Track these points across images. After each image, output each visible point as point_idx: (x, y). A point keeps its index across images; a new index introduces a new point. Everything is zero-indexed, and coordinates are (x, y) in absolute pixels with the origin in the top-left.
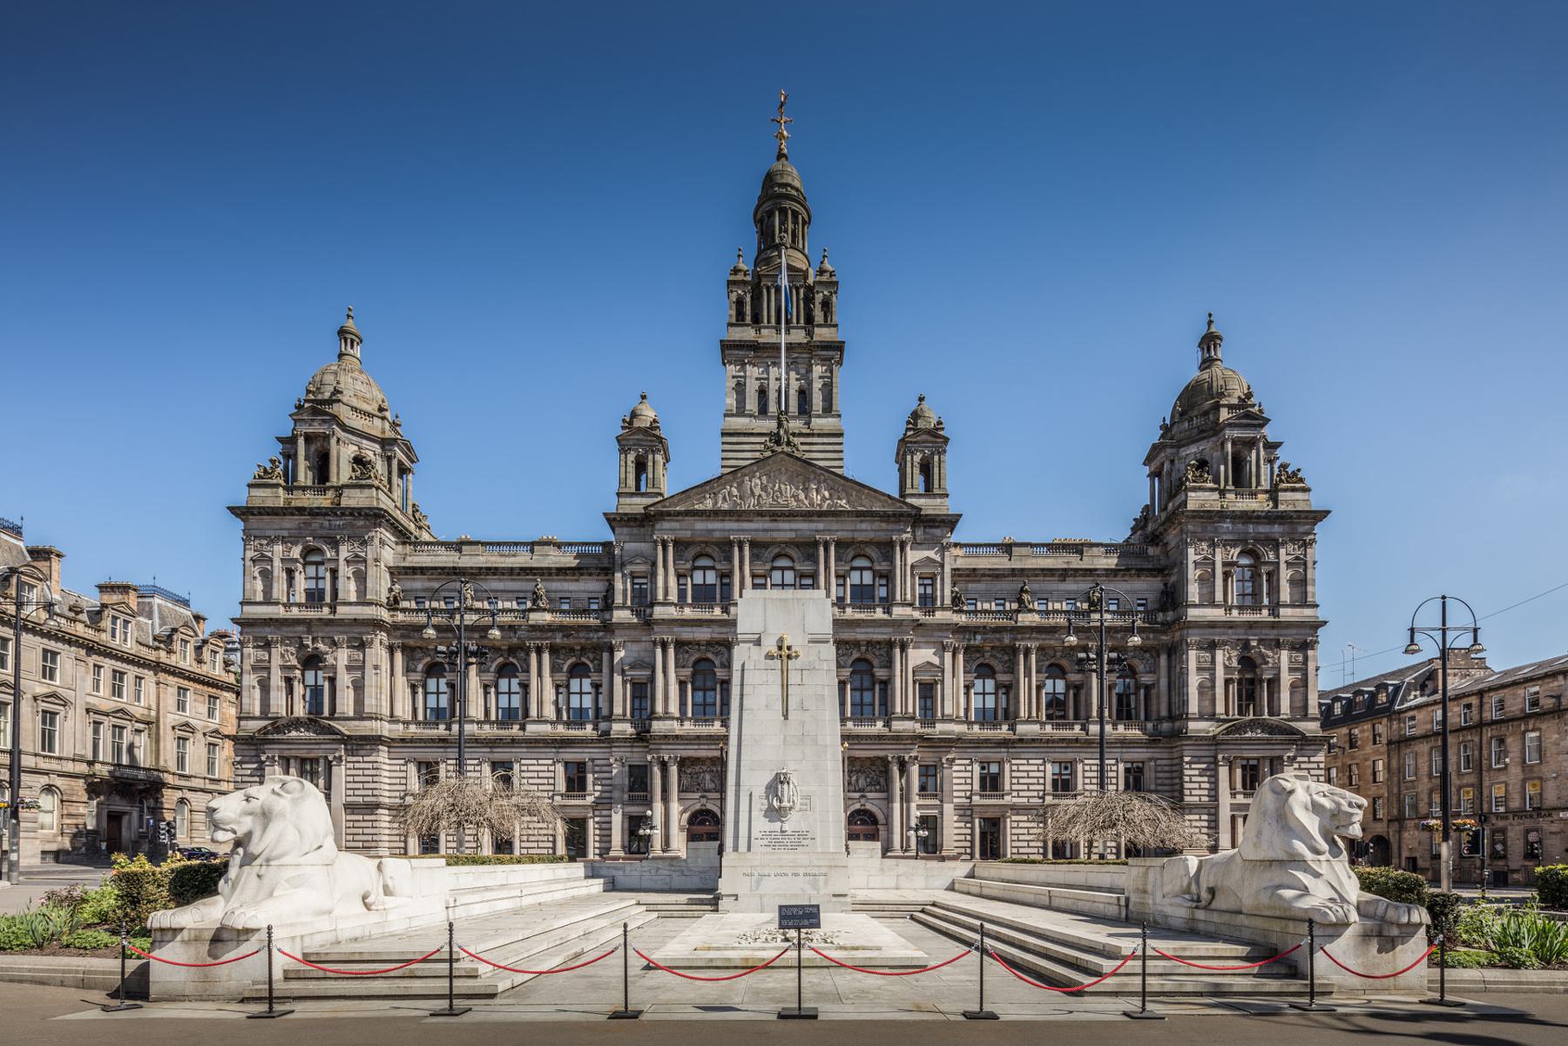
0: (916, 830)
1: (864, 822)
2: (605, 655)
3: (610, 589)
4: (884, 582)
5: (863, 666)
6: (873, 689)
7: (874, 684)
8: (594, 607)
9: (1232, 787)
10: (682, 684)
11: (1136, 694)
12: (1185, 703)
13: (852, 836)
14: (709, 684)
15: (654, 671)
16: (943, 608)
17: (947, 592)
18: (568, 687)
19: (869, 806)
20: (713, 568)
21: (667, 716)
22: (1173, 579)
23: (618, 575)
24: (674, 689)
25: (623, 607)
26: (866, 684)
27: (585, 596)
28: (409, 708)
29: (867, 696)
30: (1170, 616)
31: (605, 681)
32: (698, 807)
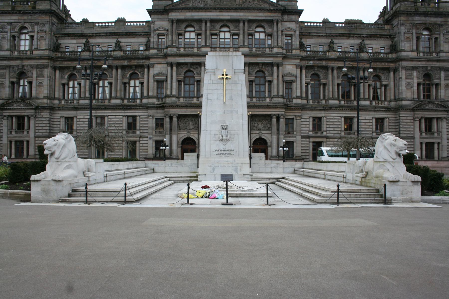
0: (283, 148)
1: (261, 144)
2: (146, 70)
3: (149, 41)
4: (270, 38)
5: (261, 74)
6: (265, 85)
7: (265, 82)
8: (141, 49)
9: (420, 130)
10: (179, 82)
11: (381, 89)
12: (401, 93)
13: (256, 151)
14: (192, 82)
15: (167, 76)
16: (296, 49)
17: (298, 43)
18: (129, 83)
19: (263, 137)
20: (194, 31)
21: (171, 96)
22: (396, 39)
23: (152, 35)
24: (175, 84)
25: (154, 49)
27: (138, 44)
28: (61, 94)
29: (262, 88)
30: (393, 56)
31: (145, 81)
32: (186, 137)
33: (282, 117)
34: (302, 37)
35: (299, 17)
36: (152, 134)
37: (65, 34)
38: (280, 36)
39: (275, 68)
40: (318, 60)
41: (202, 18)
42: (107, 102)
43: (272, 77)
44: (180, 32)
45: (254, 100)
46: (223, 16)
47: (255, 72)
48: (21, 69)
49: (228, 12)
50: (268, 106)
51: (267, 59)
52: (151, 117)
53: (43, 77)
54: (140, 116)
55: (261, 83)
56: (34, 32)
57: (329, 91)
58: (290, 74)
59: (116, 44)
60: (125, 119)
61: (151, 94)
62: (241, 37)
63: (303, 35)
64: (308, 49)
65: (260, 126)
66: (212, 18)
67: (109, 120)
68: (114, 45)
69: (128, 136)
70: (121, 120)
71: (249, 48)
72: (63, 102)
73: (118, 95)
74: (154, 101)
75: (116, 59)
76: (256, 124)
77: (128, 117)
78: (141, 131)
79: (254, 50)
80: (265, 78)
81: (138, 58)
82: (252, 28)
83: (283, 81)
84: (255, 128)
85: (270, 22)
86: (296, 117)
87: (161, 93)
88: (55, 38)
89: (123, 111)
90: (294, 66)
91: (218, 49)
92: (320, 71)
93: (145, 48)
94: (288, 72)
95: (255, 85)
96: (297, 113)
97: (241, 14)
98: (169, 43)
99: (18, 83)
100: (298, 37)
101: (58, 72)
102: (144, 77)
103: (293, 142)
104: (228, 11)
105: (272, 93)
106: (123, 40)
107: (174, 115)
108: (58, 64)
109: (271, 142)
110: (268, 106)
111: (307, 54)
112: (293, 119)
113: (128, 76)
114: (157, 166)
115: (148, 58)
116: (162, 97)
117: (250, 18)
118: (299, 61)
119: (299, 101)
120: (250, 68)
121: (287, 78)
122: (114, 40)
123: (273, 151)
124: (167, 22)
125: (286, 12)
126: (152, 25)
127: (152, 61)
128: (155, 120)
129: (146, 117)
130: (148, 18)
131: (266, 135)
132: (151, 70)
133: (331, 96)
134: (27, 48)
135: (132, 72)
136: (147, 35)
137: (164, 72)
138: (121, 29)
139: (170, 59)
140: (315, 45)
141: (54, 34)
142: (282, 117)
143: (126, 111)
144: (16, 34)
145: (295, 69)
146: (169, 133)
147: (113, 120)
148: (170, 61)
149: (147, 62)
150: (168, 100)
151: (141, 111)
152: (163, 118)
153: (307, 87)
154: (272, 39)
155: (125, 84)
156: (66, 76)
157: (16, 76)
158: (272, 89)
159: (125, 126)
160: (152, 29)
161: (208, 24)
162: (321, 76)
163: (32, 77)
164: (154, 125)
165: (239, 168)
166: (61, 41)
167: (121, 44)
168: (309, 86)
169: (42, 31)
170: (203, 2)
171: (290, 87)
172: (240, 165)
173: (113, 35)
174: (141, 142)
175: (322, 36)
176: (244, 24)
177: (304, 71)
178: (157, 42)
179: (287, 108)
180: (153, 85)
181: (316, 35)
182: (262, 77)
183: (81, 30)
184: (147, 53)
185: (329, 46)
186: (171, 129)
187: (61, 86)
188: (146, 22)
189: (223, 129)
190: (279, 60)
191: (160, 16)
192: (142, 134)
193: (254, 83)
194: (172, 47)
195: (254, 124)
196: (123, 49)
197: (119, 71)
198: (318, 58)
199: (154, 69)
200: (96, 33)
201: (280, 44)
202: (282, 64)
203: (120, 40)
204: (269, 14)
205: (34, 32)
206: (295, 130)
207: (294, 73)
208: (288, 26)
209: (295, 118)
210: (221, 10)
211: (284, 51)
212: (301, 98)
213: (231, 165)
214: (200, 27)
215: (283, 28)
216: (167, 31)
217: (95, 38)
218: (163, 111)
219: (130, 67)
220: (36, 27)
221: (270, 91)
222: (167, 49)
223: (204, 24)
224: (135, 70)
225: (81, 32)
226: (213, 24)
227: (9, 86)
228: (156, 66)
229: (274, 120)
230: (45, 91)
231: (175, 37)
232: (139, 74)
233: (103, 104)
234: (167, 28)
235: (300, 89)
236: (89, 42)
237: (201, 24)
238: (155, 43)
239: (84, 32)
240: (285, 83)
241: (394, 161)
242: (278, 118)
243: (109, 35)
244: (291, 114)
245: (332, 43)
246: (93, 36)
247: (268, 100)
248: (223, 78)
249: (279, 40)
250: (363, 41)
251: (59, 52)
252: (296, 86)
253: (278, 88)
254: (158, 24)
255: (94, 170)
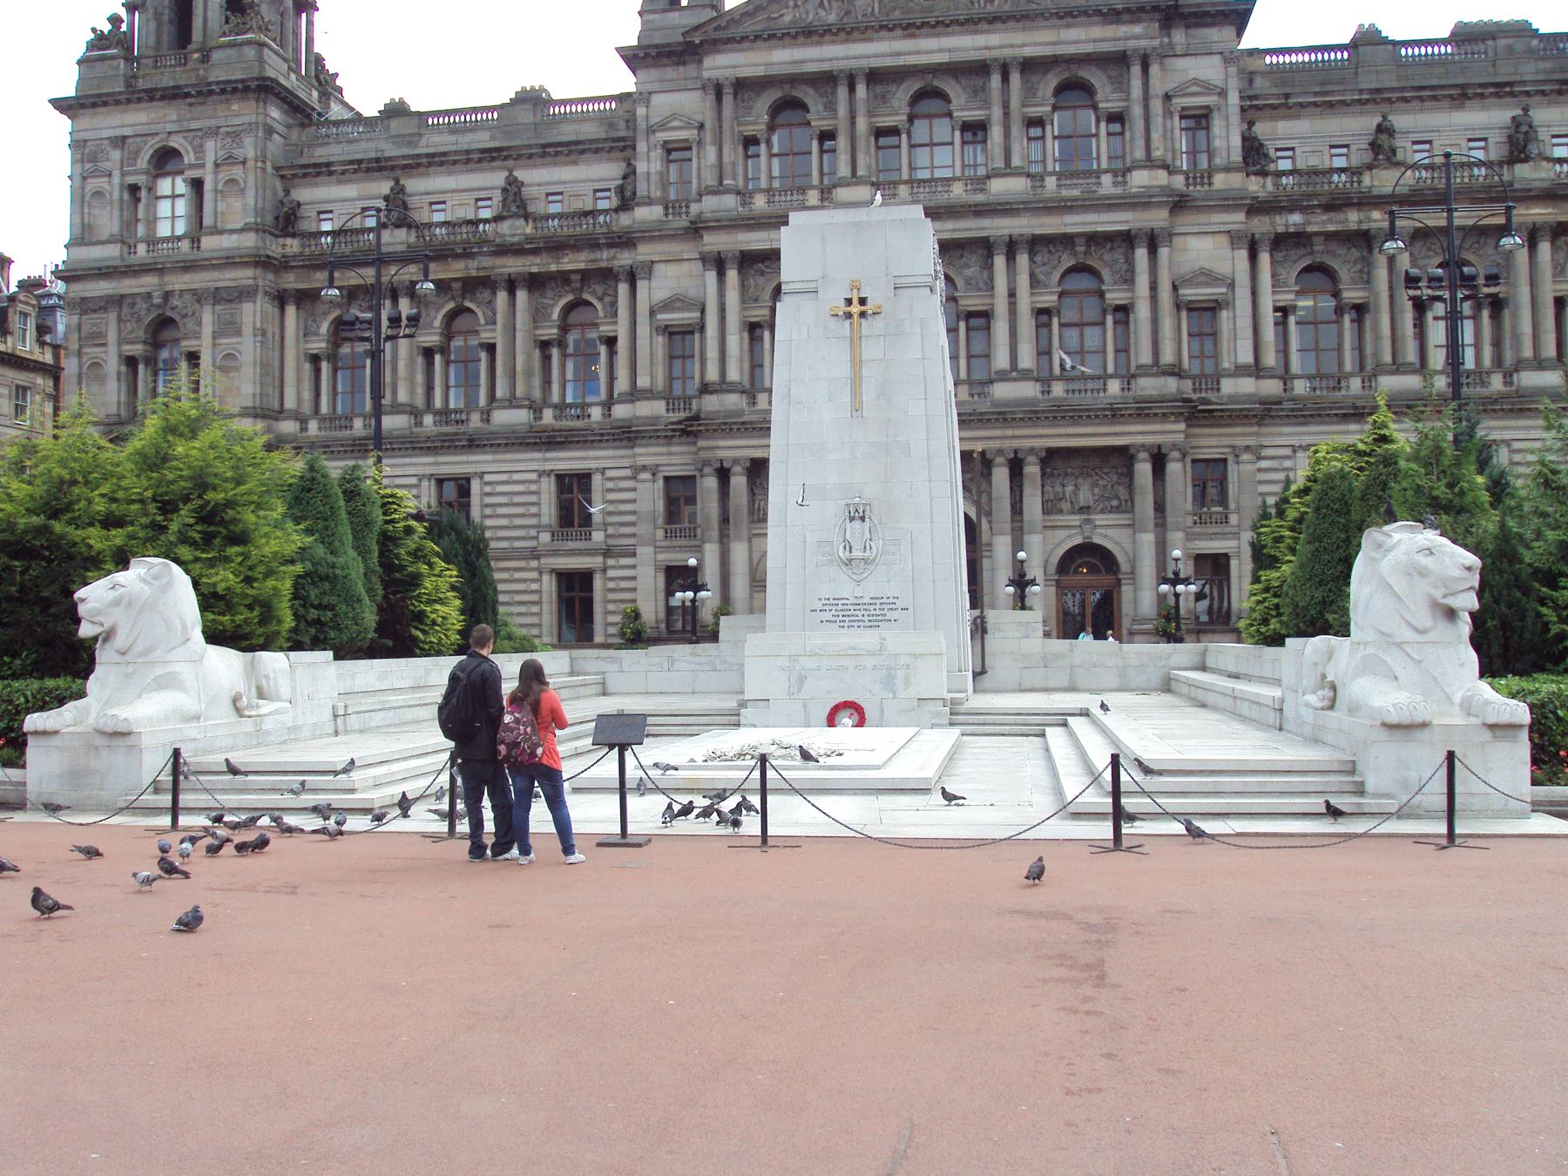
2: (623, 288)
3: (630, 174)
4: (1116, 127)
5: (1083, 282)
6: (1103, 324)
7: (1104, 312)
8: (603, 205)
15: (703, 311)
16: (1227, 169)
17: (1237, 141)
19: (1097, 540)
21: (724, 386)
23: (642, 147)
25: (650, 202)
26: (1091, 313)
28: (307, 395)
29: (1092, 334)
33: (1175, 454)
34: (1251, 114)
35: (1240, 33)
36: (653, 542)
37: (315, 165)
38: (1160, 120)
39: (1141, 254)
40: (1329, 207)
41: (834, 66)
42: (475, 420)
43: (1132, 290)
44: (750, 130)
45: (1058, 389)
46: (918, 53)
47: (1057, 275)
48: (158, 306)
49: (938, 35)
50: (1114, 414)
51: (1104, 217)
52: (645, 476)
53: (239, 333)
54: (603, 471)
55: (1085, 320)
56: (202, 166)
57: (1377, 338)
58: (1207, 276)
59: (504, 190)
60: (548, 487)
61: (643, 382)
62: (996, 133)
63: (1258, 108)
64: (1285, 165)
65: (1085, 496)
66: (875, 63)
67: (488, 489)
68: (497, 196)
69: (555, 553)
70: (533, 487)
71: (1028, 175)
72: (313, 426)
73: (520, 391)
74: (657, 408)
75: (503, 250)
76: (1069, 489)
77: (440, 482)
78: (611, 530)
79: (1051, 182)
80: (1101, 294)
81: (592, 244)
82: (1040, 93)
83: (1178, 307)
84: (1065, 506)
85: (1118, 61)
86: (1236, 452)
87: (684, 379)
88: (278, 184)
89: (538, 455)
90: (1223, 240)
91: (903, 190)
92: (1333, 254)
93: (615, 202)
94: (1197, 266)
95: (1061, 325)
96: (1242, 436)
97: (994, 39)
98: (710, 180)
99: (151, 361)
100: (1235, 118)
101: (291, 310)
102: (615, 315)
103: (1226, 556)
104: (940, 29)
105: (1133, 358)
106: (534, 177)
107: (736, 461)
108: (291, 281)
109: (1133, 562)
110: (1114, 414)
111: (1277, 185)
112: (1225, 460)
113: (555, 316)
114: (616, 667)
115: (626, 241)
116: (690, 392)
117: (1029, 52)
118: (1240, 217)
119: (1247, 385)
120: (1038, 258)
121: (1189, 293)
122: (497, 178)
123: (1142, 597)
124: (697, 95)
125: (1183, 16)
126: (641, 111)
127: (645, 252)
128: (660, 483)
129: (627, 473)
130: (624, 81)
131: (1109, 532)
132: (642, 285)
133: (1388, 358)
134: (180, 229)
135: (570, 297)
136: (624, 149)
137: (693, 293)
138: (528, 130)
139: (715, 242)
140: (1311, 143)
141: (277, 169)
142: (1175, 454)
143: (549, 455)
144: (141, 180)
145: (1227, 252)
146: (715, 534)
147: (500, 489)
148: (715, 248)
149: (624, 259)
150: (711, 403)
151: (611, 453)
152: (694, 477)
153: (1282, 324)
154: (1128, 134)
155: (545, 346)
156: (325, 327)
157: (141, 333)
158: (1132, 341)
159: (548, 510)
160: (641, 125)
161: (861, 90)
162: (1344, 274)
163: (197, 335)
164: (660, 505)
165: (900, 673)
166: (303, 194)
167: (525, 191)
168: (1292, 319)
169: (230, 160)
170: (835, 5)
171: (1207, 330)
172: (902, 661)
173: (493, 159)
174: (611, 573)
175: (1343, 103)
176: (1005, 78)
177: (1265, 258)
178: (661, 174)
179: (1196, 414)
180: (651, 347)
181: (1315, 104)
182: (1087, 292)
183: (371, 145)
184: (625, 220)
185: (1375, 146)
186: (725, 520)
187: (307, 366)
188: (622, 98)
189: (852, 519)
190: (1157, 218)
191: (671, 73)
192: (611, 542)
193: (1055, 321)
194: (719, 190)
195: (1059, 489)
196: (531, 209)
197: (522, 295)
198: (1324, 201)
199: (654, 283)
200: (428, 155)
201: (1157, 154)
202: (1171, 235)
203: (520, 174)
204: (1110, 31)
205: (202, 166)
206: (1232, 505)
207: (1222, 267)
208: (1192, 74)
209: (1231, 459)
210: (911, 28)
211: (1179, 182)
212: (1257, 370)
213: (869, 662)
214: (831, 107)
215: (1169, 86)
216: (701, 127)
217: (428, 175)
218: (692, 449)
219: (563, 278)
220: (210, 145)
221: (1123, 350)
222: (700, 201)
223: (842, 92)
224: (581, 289)
225: (373, 155)
226: (879, 89)
227: (119, 374)
228: (660, 269)
229: (1144, 469)
230: (246, 387)
231: (732, 153)
232: (599, 306)
233: (462, 428)
234: (699, 118)
235: (1249, 333)
236: (402, 190)
237: (834, 93)
238: (654, 178)
239: (387, 154)
240: (1184, 314)
241: (1419, 638)
242: (1159, 461)
243: (480, 160)
244: (1214, 441)
245: (1384, 129)
246: (418, 165)
247: (1114, 387)
248: (849, 316)
249: (1156, 136)
250: (1526, 110)
251: (294, 235)
252: (1235, 326)
253: (1160, 335)
254: (663, 103)
255: (285, 691)
